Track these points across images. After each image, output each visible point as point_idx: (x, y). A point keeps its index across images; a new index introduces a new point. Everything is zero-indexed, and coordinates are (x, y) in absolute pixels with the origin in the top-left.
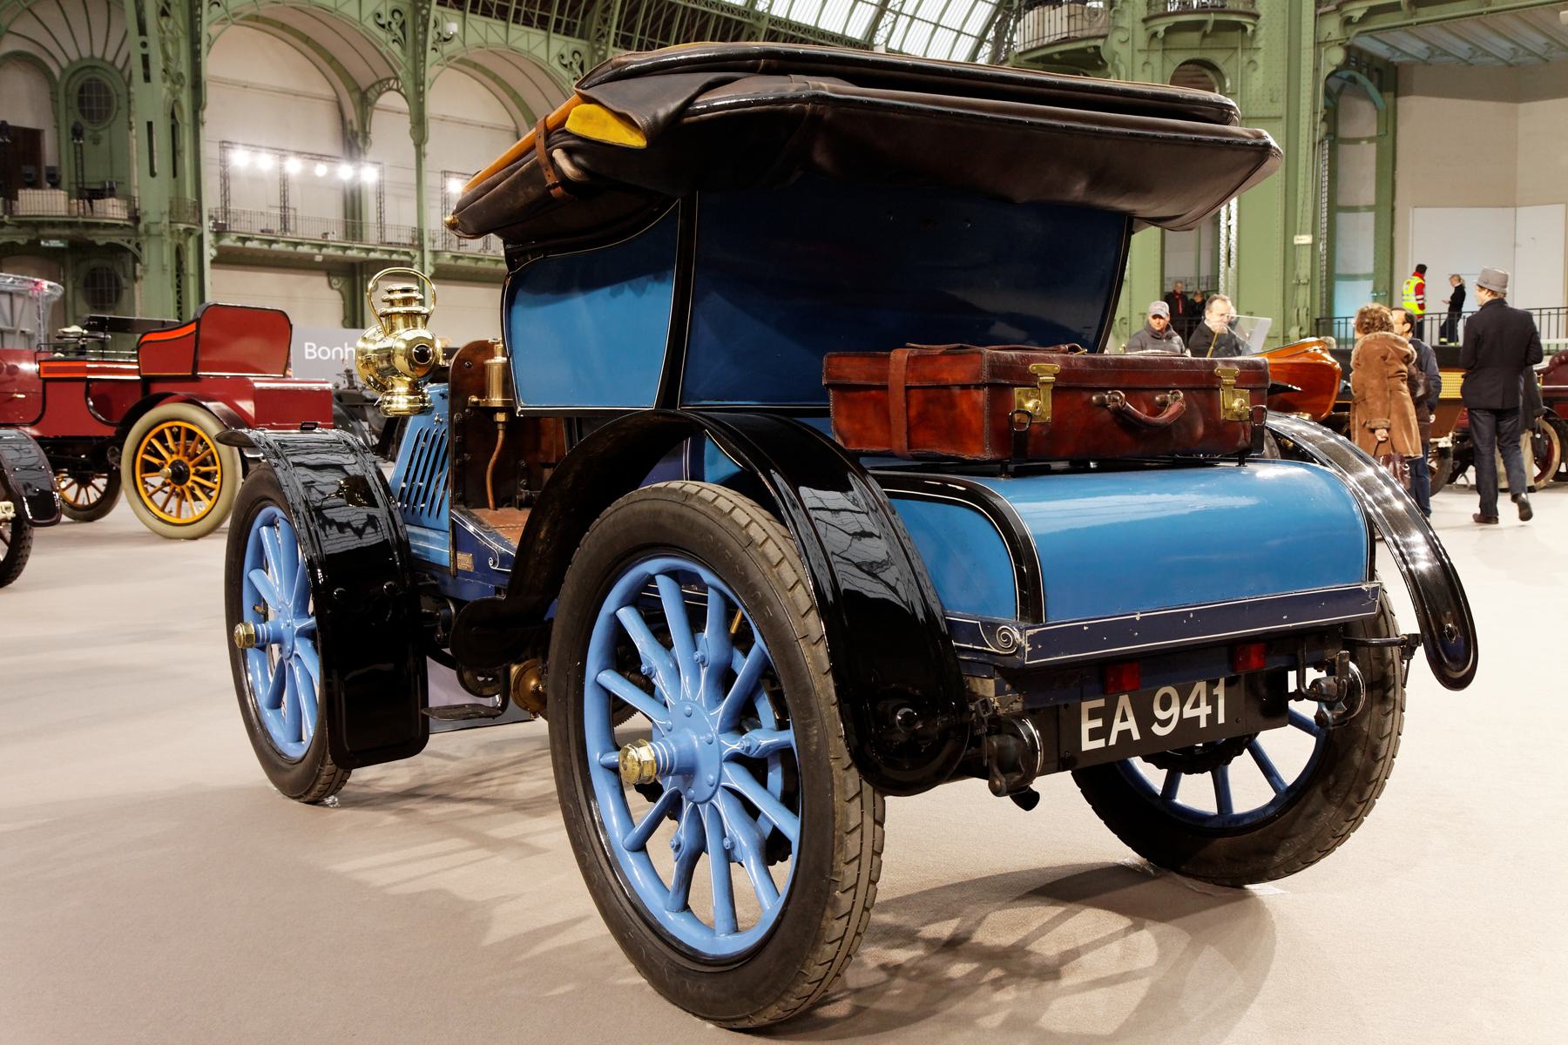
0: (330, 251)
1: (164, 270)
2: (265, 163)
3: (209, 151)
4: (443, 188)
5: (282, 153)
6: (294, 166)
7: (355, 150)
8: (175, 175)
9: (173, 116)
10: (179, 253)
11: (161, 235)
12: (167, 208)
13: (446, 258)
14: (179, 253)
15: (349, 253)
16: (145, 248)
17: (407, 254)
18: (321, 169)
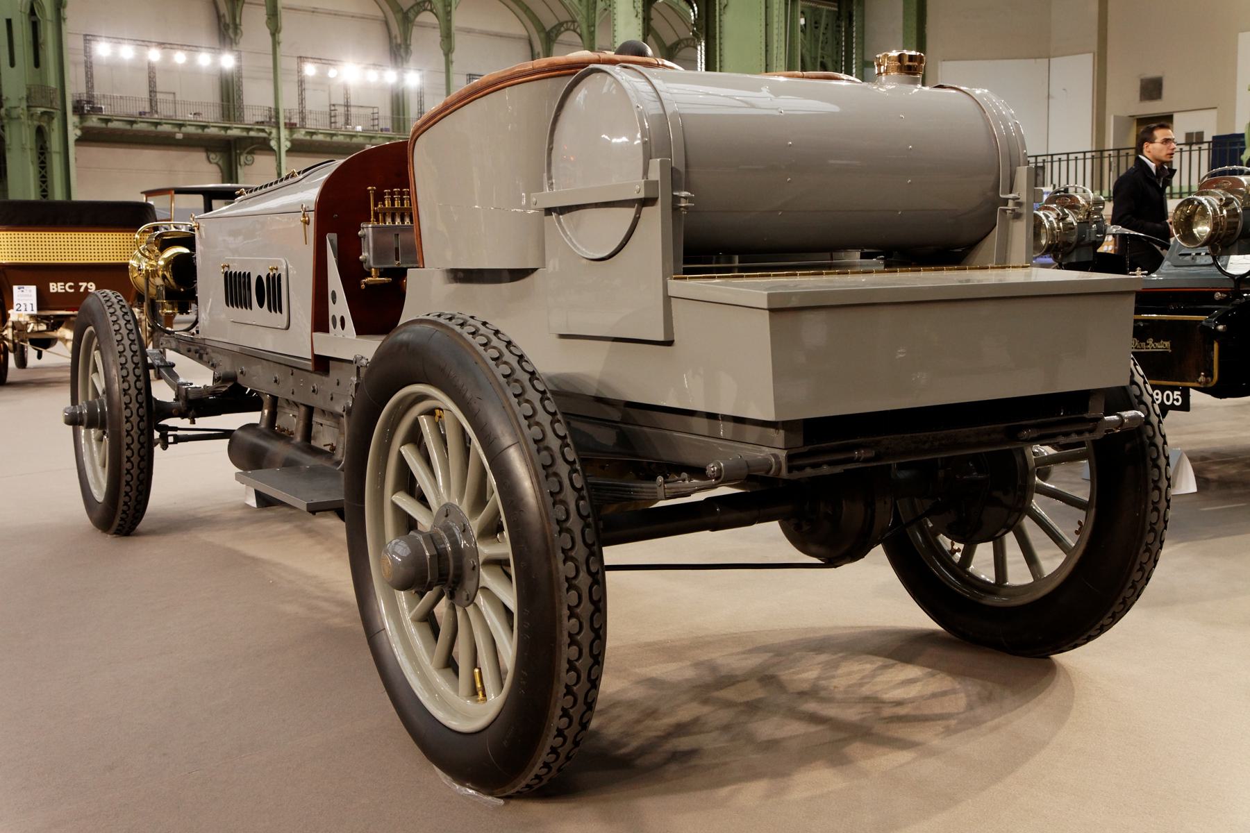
0: (191, 130)
1: (23, 149)
2: (127, 52)
3: (72, 42)
4: (300, 71)
5: (145, 43)
6: (155, 55)
7: (228, 40)
8: (37, 64)
9: (32, 12)
10: (40, 133)
11: (19, 118)
12: (24, 94)
13: (300, 135)
14: (40, 133)
15: (230, 132)
16: (7, 129)
17: (263, 131)
18: (180, 58)
